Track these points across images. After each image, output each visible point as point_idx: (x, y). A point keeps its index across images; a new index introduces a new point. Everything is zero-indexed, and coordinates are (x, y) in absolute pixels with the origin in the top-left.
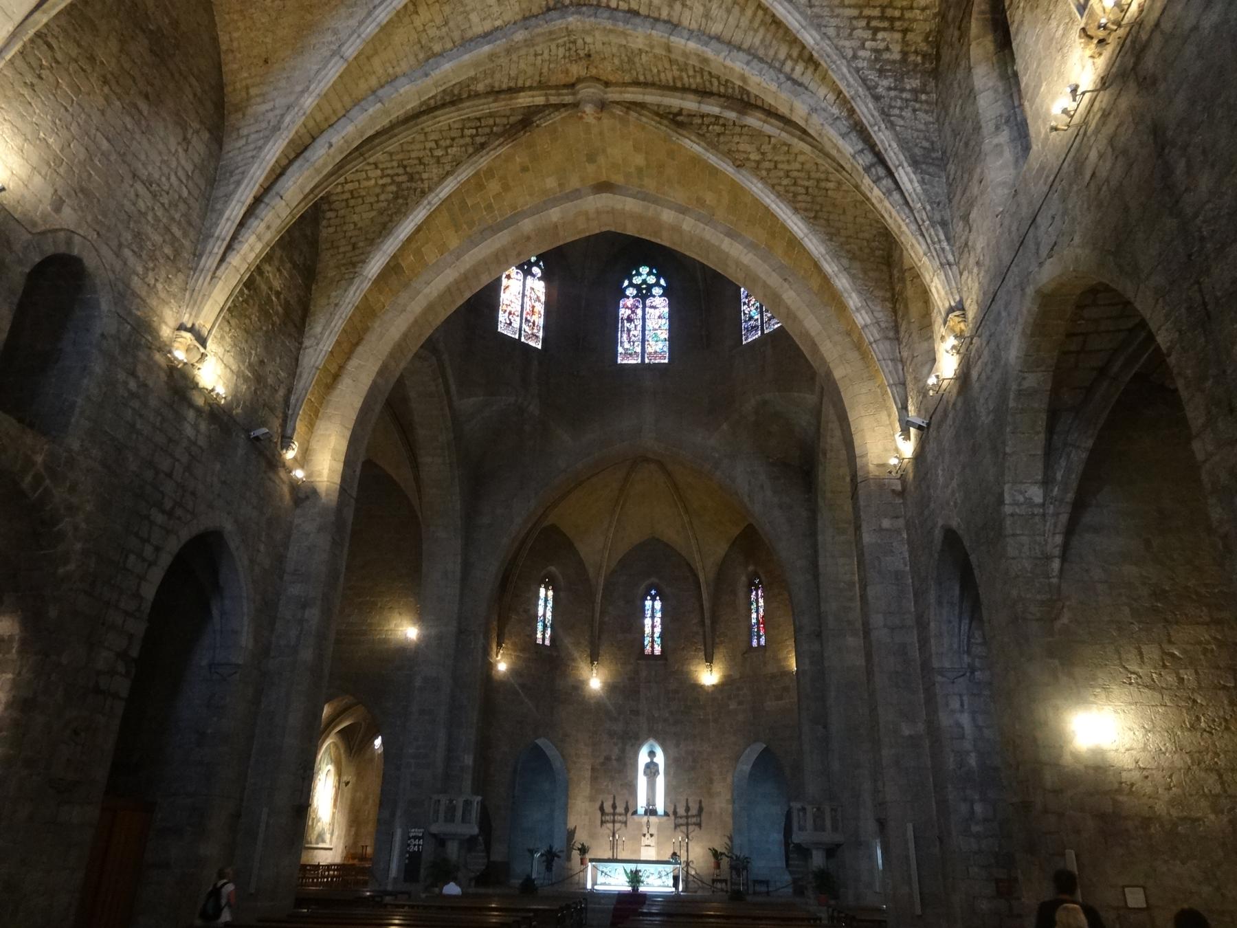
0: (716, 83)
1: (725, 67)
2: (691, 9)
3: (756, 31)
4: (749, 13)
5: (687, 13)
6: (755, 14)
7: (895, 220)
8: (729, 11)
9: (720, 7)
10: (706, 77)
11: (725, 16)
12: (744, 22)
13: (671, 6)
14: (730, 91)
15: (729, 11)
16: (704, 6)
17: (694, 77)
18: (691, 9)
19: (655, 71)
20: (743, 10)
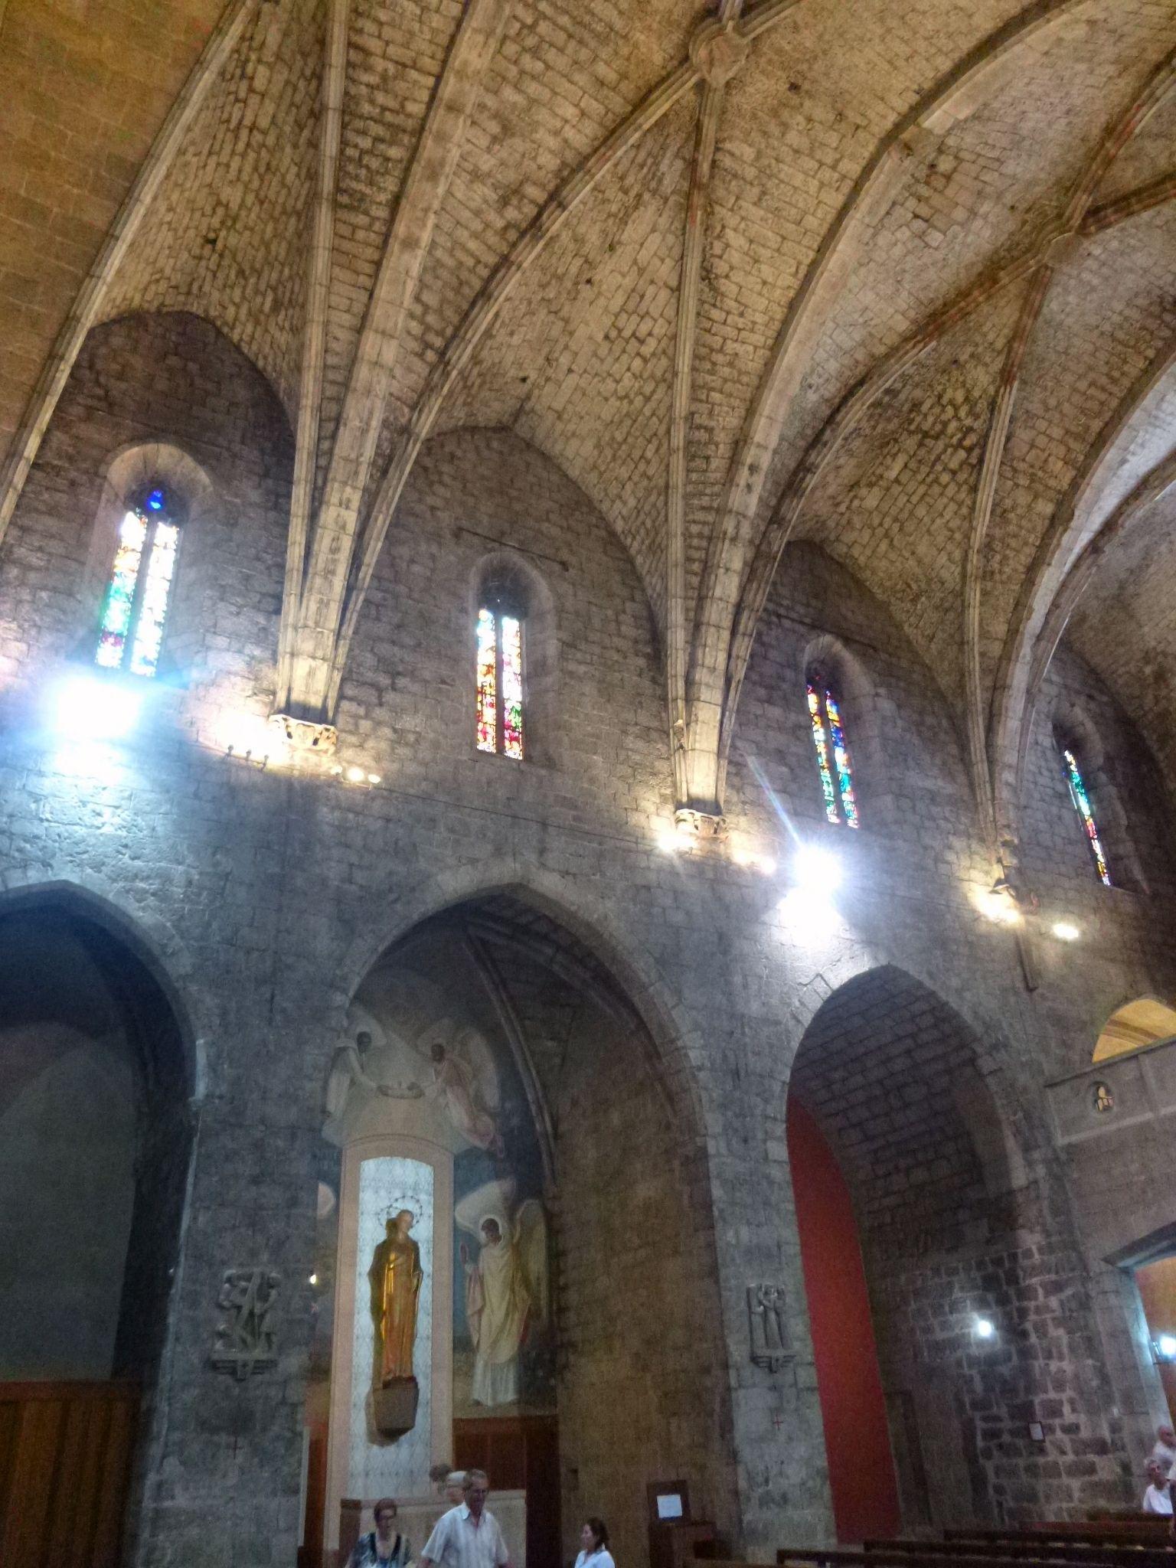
0: (365, 143)
1: (426, 210)
2: (489, 150)
3: (451, 252)
4: (472, 245)
5: (484, 142)
6: (472, 255)
7: (334, 561)
8: (477, 213)
9: (486, 201)
10: (377, 130)
11: (473, 205)
12: (463, 235)
13: (496, 116)
14: (351, 168)
15: (477, 213)
16: (489, 174)
17: (372, 102)
18: (489, 150)
19: (383, 15)
20: (475, 235)
